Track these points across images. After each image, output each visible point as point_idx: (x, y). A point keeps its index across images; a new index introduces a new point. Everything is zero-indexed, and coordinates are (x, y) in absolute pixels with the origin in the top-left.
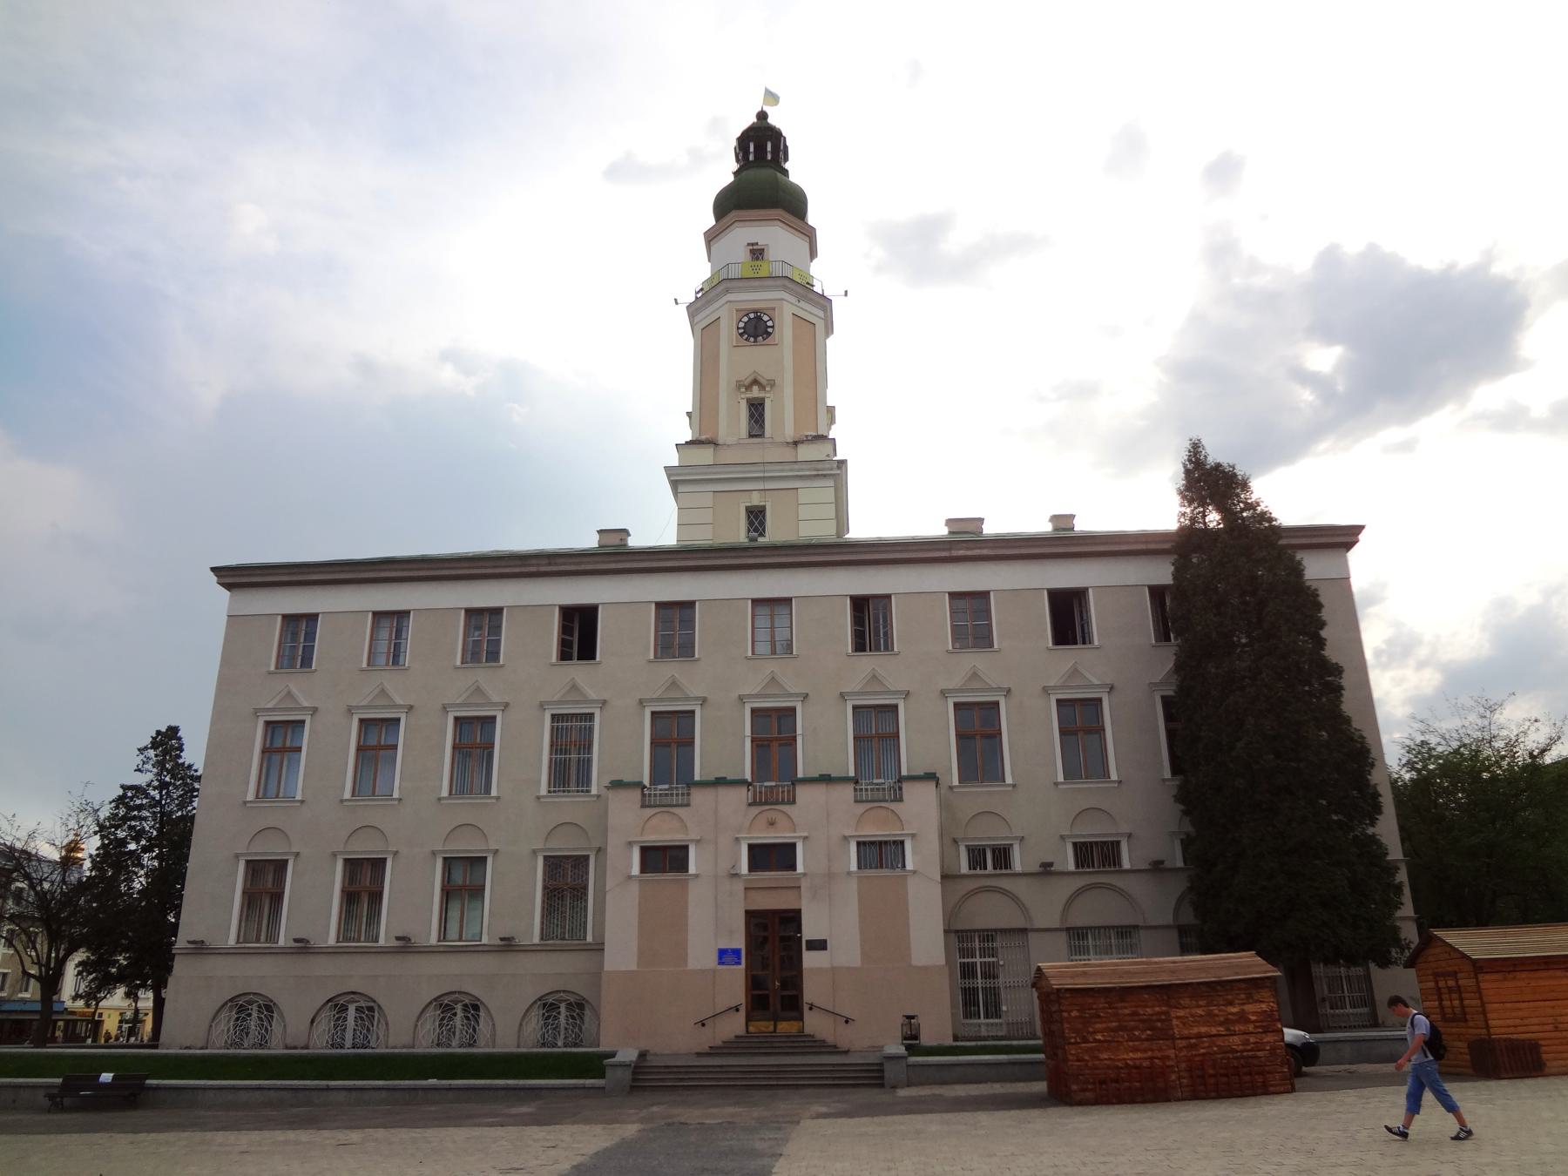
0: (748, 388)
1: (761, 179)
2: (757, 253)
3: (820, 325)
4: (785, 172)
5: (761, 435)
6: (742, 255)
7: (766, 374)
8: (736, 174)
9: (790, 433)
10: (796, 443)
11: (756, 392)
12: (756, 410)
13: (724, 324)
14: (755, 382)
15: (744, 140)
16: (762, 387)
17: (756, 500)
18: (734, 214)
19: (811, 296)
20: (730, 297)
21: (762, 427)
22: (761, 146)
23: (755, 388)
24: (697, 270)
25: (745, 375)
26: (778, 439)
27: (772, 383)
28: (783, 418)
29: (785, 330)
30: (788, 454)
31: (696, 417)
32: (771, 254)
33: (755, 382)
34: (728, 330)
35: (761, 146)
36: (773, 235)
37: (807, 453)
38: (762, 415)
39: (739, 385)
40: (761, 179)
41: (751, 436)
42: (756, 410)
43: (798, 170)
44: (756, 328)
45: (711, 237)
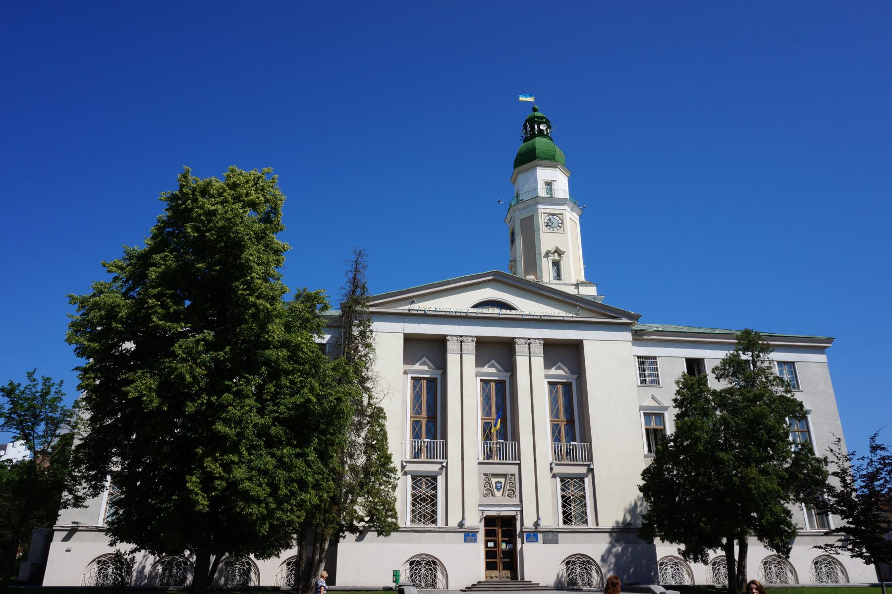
7: (562, 249)
11: (556, 257)
12: (556, 264)
33: (556, 251)
42: (556, 264)
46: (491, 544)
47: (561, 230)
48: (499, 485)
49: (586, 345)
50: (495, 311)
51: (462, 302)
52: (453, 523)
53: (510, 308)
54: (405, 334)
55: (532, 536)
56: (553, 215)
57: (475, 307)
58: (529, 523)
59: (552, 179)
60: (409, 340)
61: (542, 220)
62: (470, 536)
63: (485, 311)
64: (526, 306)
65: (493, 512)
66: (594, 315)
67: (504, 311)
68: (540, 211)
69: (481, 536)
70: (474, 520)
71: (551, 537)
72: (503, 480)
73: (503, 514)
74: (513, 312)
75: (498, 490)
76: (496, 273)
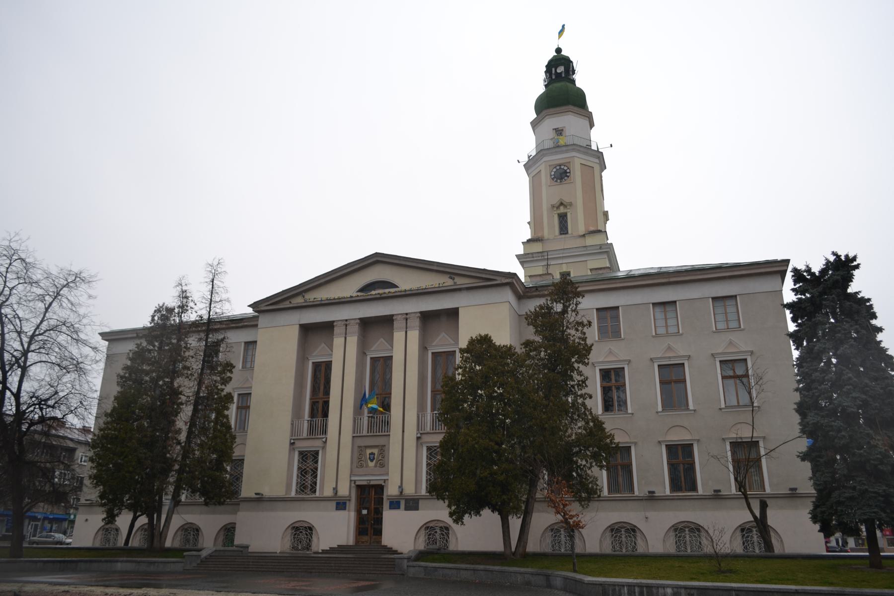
0: (558, 208)
1: (561, 91)
2: (559, 132)
3: (597, 168)
4: (573, 82)
5: (567, 233)
6: (552, 134)
7: (566, 200)
8: (546, 86)
9: (582, 230)
10: (584, 236)
11: (562, 210)
12: (563, 218)
13: (543, 174)
14: (562, 204)
15: (551, 66)
16: (565, 206)
18: (544, 112)
19: (590, 152)
20: (545, 159)
21: (567, 228)
22: (560, 69)
23: (562, 208)
24: (528, 144)
25: (555, 201)
26: (575, 234)
27: (571, 204)
28: (578, 223)
29: (577, 173)
30: (580, 242)
31: (532, 224)
32: (567, 132)
33: (562, 204)
34: (545, 178)
35: (560, 69)
36: (568, 121)
37: (591, 241)
38: (566, 222)
39: (553, 206)
40: (561, 91)
41: (561, 234)
42: (563, 218)
43: (581, 80)
44: (562, 175)
45: (535, 124)
46: (365, 512)
48: (372, 456)
49: (460, 310)
51: (349, 288)
52: (328, 492)
55: (395, 505)
57: (361, 290)
58: (392, 490)
60: (307, 330)
62: (341, 505)
64: (406, 281)
65: (363, 480)
69: (352, 505)
70: (344, 490)
71: (412, 504)
72: (376, 451)
73: (372, 483)
74: (392, 290)
75: (372, 461)
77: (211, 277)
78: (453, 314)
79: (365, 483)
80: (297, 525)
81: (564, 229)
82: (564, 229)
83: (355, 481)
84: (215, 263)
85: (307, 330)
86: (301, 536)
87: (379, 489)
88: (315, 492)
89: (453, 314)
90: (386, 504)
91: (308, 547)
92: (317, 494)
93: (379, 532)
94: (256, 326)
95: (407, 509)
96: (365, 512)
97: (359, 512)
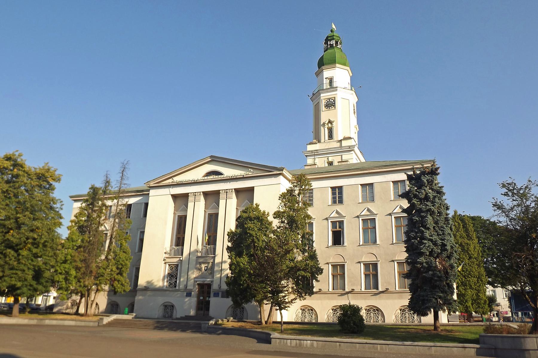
12: (330, 131)
17: (330, 159)
47: (333, 108)
50: (211, 178)
53: (220, 174)
54: (171, 195)
55: (216, 295)
56: (329, 99)
57: (204, 176)
58: (215, 287)
59: (340, 75)
61: (323, 103)
62: (189, 295)
63: (211, 177)
64: (228, 172)
66: (259, 172)
67: (219, 176)
68: (321, 98)
76: (211, 157)
77: (122, 169)
78: (251, 190)
79: (202, 282)
80: (165, 304)
81: (331, 136)
82: (331, 136)
83: (196, 281)
84: (125, 162)
85: (175, 197)
86: (167, 310)
87: (209, 286)
88: (175, 287)
89: (251, 190)
90: (212, 294)
91: (171, 316)
92: (177, 288)
93: (208, 309)
94: (149, 194)
95: (222, 297)
96: (202, 298)
97: (198, 297)
